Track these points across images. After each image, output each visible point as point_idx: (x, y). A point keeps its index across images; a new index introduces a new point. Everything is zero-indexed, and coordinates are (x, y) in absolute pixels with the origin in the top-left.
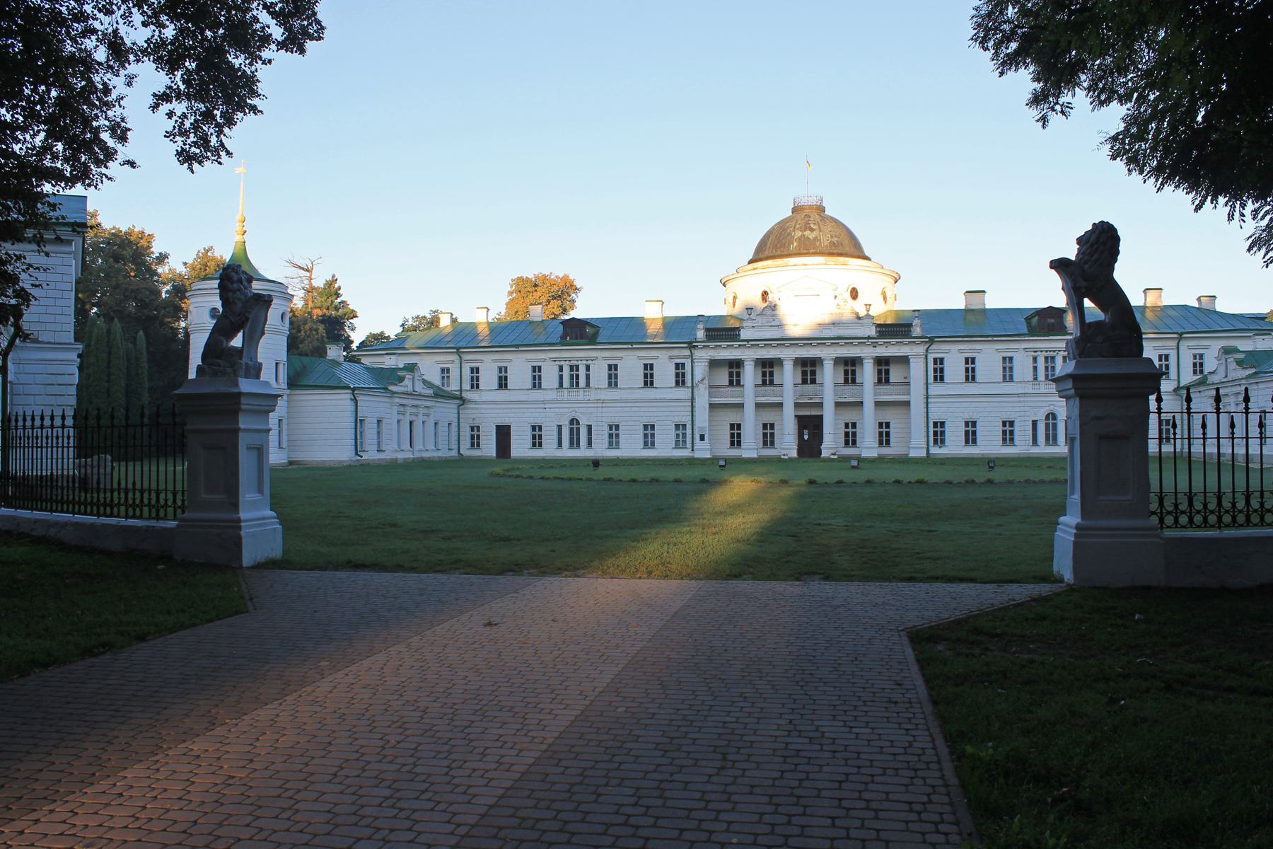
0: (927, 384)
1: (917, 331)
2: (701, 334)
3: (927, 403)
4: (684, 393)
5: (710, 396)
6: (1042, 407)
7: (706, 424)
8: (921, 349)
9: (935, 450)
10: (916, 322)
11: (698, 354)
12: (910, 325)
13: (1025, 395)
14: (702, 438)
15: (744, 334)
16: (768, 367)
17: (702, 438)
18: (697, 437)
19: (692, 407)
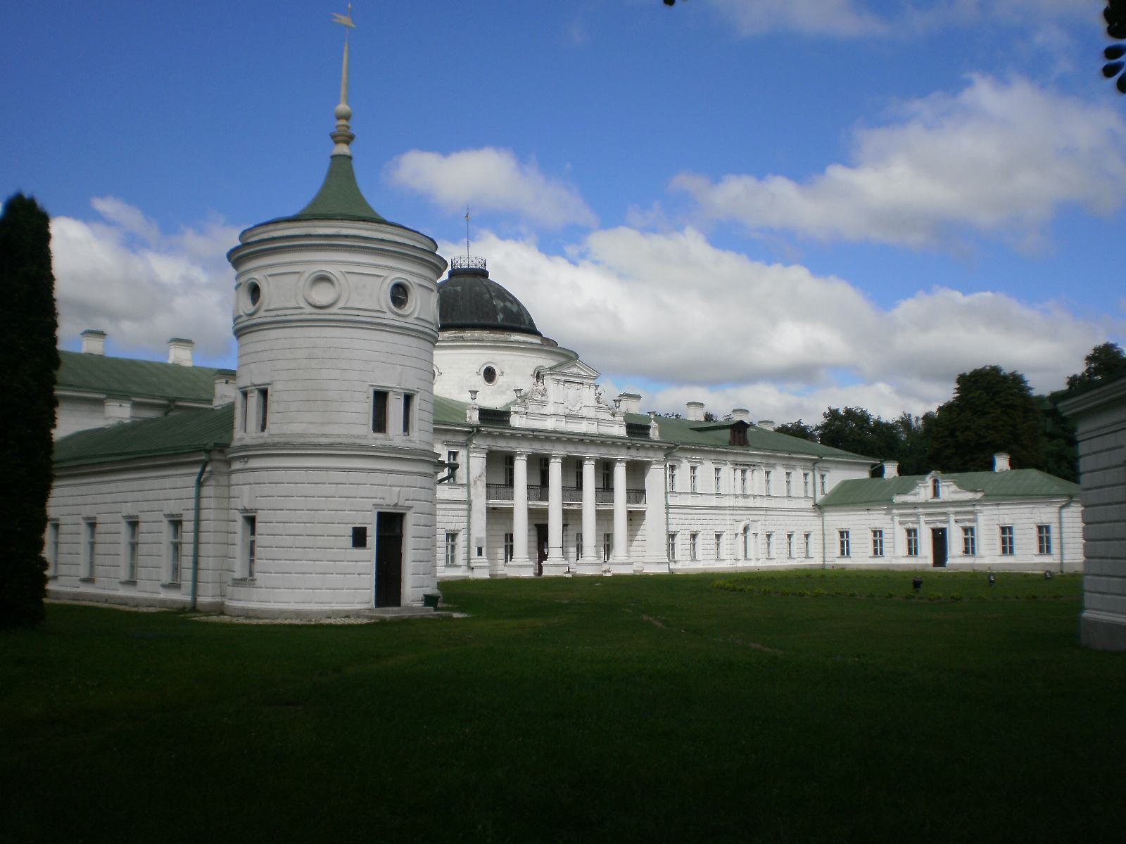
0: (666, 493)
1: (654, 434)
2: (474, 417)
3: (667, 513)
4: (460, 494)
5: (488, 498)
6: (741, 520)
7: (483, 534)
8: (661, 456)
9: (673, 566)
10: (653, 424)
11: (476, 441)
12: (649, 428)
13: (733, 508)
14: (480, 553)
15: (516, 421)
16: (540, 465)
17: (480, 553)
18: (475, 551)
19: (469, 510)
